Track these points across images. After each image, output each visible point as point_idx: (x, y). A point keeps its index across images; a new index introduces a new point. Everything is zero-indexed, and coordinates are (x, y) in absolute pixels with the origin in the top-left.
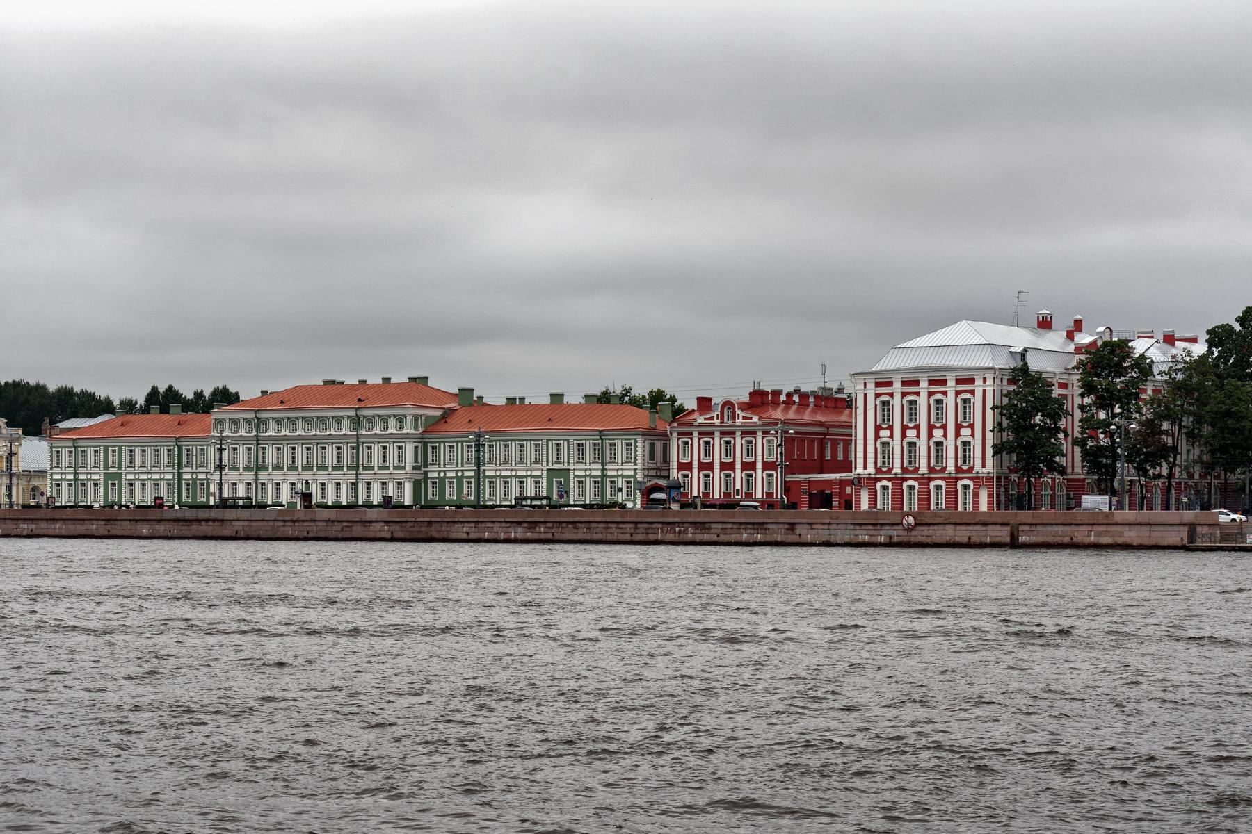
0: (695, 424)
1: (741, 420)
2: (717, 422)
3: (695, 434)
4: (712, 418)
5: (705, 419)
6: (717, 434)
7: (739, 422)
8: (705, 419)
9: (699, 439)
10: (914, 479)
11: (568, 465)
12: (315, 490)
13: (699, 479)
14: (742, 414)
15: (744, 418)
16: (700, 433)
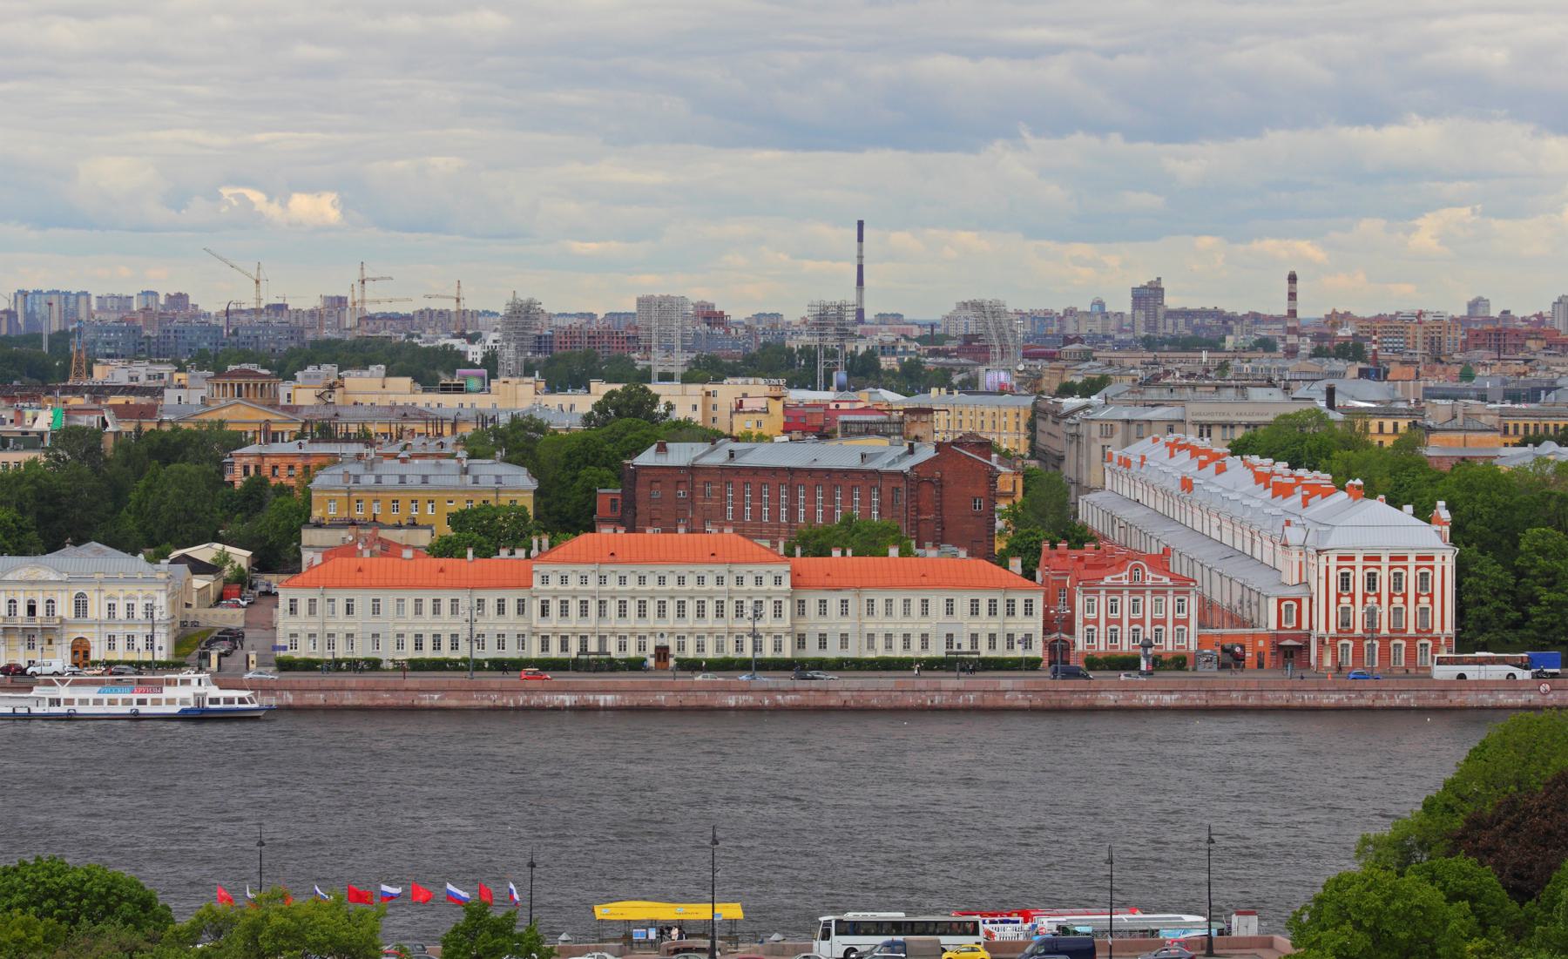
0: (1102, 583)
1: (1150, 581)
2: (1126, 582)
3: (1103, 593)
4: (1121, 578)
5: (1113, 579)
6: (1126, 593)
7: (1148, 582)
8: (1113, 579)
9: (1106, 597)
10: (1349, 639)
11: (962, 618)
12: (672, 643)
13: (1106, 632)
14: (1151, 575)
15: (1153, 579)
16: (1107, 592)
